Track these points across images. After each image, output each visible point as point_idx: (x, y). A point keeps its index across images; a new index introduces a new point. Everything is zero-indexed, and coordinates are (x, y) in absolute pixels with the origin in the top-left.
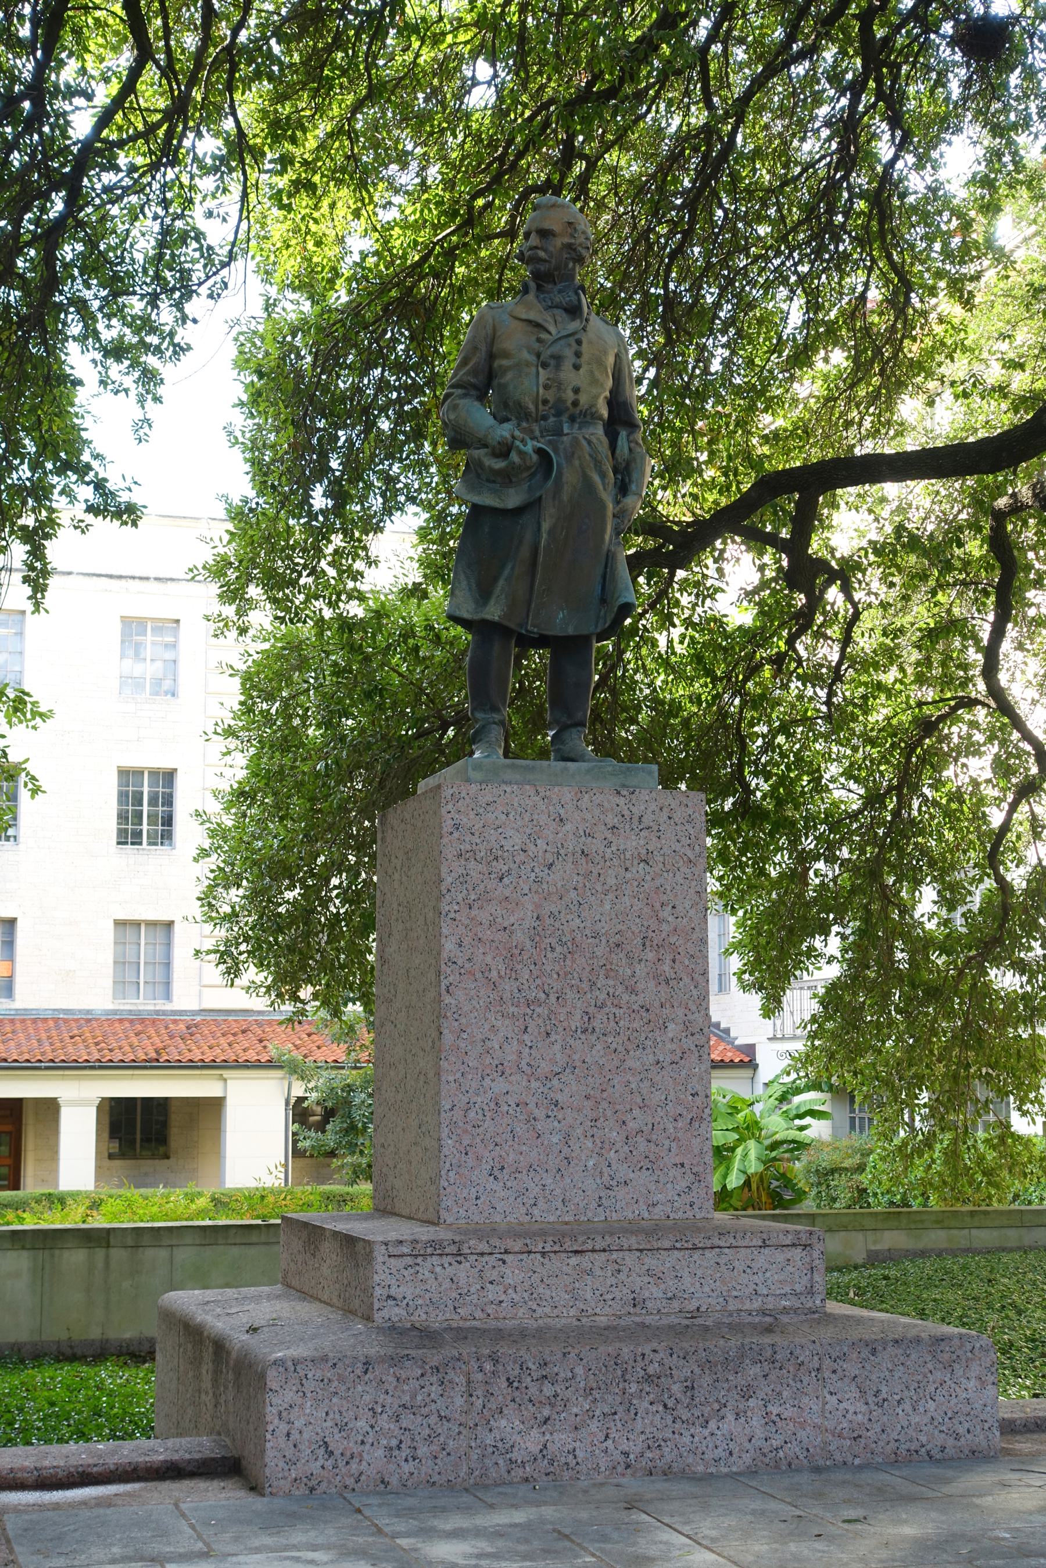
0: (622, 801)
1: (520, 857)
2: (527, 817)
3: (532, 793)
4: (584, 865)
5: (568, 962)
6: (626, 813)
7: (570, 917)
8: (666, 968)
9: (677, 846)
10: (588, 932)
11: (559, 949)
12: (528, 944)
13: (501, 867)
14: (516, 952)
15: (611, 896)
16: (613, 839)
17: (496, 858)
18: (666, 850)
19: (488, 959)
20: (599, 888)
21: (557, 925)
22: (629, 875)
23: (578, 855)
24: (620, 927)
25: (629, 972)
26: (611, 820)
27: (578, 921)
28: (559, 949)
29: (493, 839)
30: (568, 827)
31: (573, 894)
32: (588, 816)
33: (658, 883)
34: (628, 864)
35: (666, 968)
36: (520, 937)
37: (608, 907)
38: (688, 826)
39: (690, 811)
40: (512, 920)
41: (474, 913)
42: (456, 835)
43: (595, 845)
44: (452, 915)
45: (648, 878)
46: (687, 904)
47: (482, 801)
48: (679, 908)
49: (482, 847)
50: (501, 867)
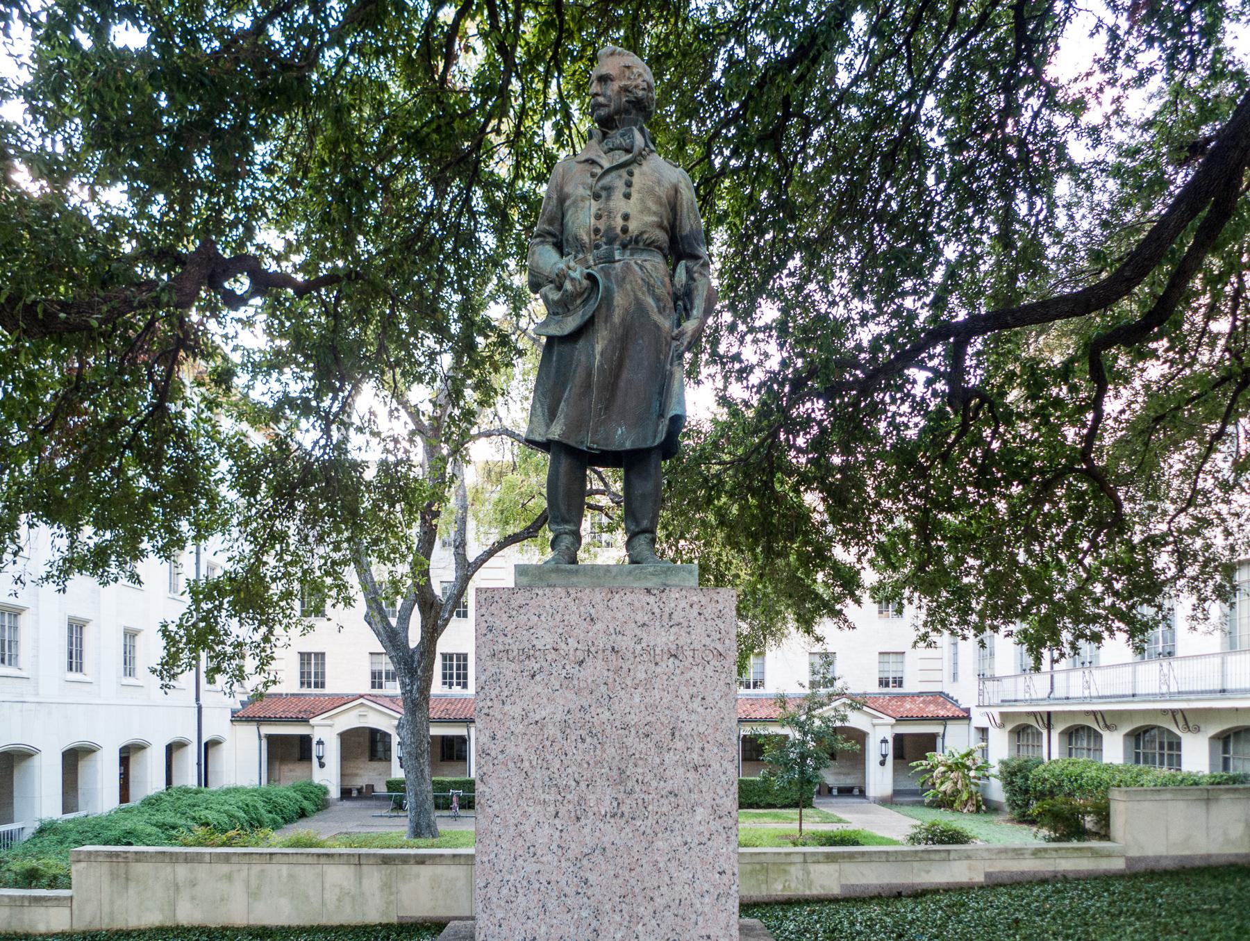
0: (652, 599)
1: (551, 656)
2: (558, 617)
3: (563, 594)
4: (615, 662)
5: (598, 752)
6: (657, 611)
7: (599, 711)
8: (695, 756)
9: (708, 641)
10: (617, 724)
11: (589, 740)
12: (559, 735)
13: (533, 665)
14: (548, 743)
15: (640, 690)
16: (644, 636)
17: (528, 657)
18: (696, 645)
19: (521, 751)
20: (629, 683)
21: (588, 717)
22: (658, 670)
23: (608, 652)
24: (648, 719)
25: (658, 760)
26: (641, 617)
27: (608, 714)
28: (589, 740)
29: (525, 638)
30: (599, 626)
31: (603, 688)
32: (619, 615)
33: (688, 675)
34: (658, 659)
35: (695, 756)
36: (552, 731)
37: (637, 700)
38: (719, 622)
39: (720, 607)
40: (544, 713)
41: (507, 708)
42: (490, 636)
43: (625, 643)
44: (486, 711)
45: (678, 672)
46: (717, 695)
47: (514, 604)
48: (709, 699)
49: (515, 648)
50: (533, 665)
